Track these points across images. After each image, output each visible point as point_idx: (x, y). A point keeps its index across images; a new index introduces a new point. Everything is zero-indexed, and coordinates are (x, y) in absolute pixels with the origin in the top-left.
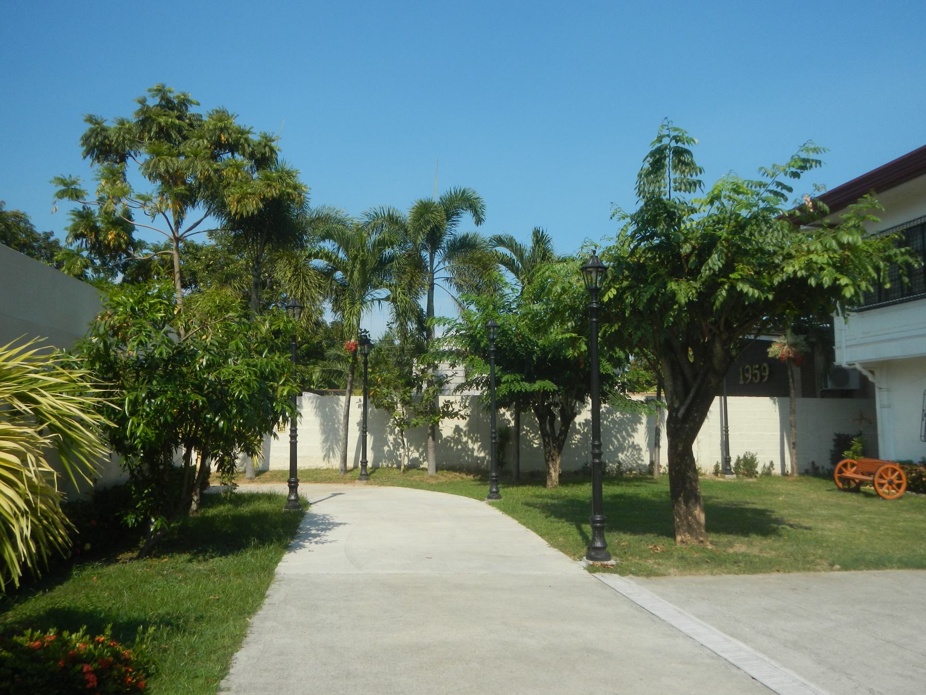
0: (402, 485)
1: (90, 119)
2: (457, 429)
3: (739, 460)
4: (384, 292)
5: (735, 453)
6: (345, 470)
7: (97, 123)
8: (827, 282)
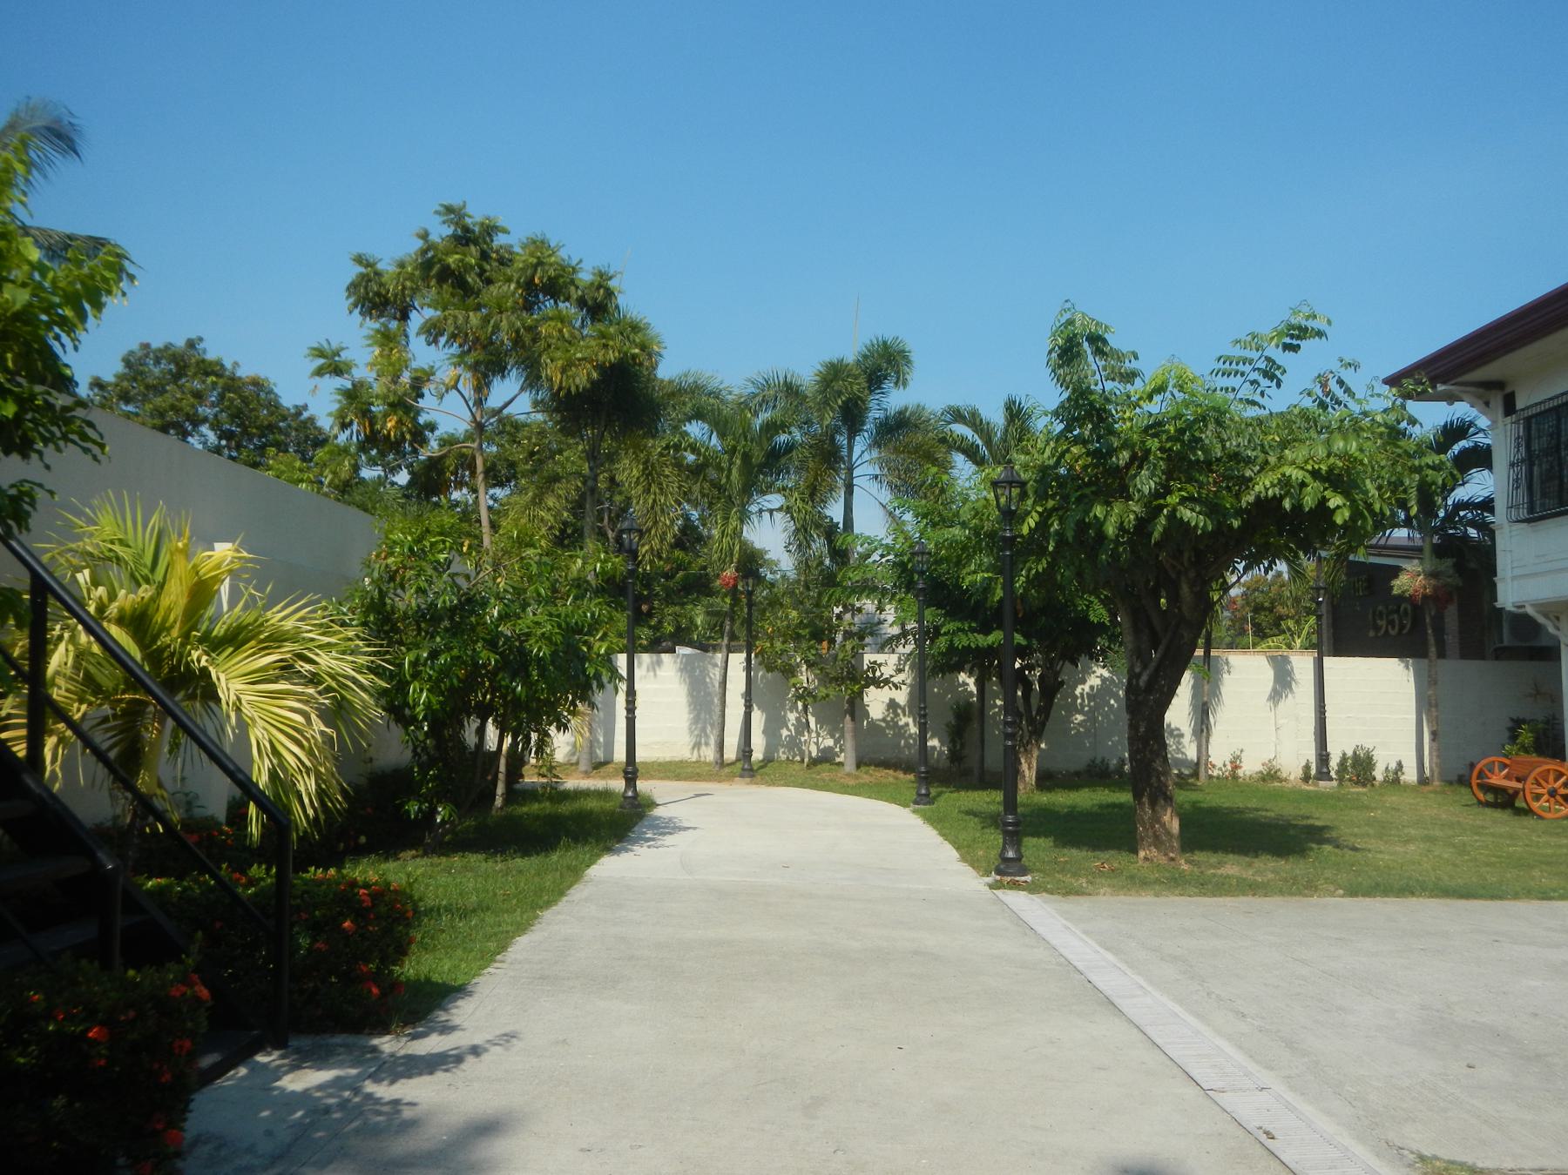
0: (802, 786)
1: (359, 260)
2: (892, 705)
3: (1344, 758)
4: (775, 500)
5: (1335, 752)
6: (721, 763)
7: (368, 265)
8: (1309, 502)
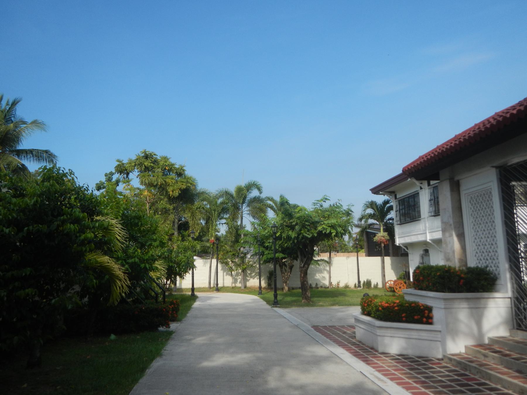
0: (231, 292)
1: (118, 161)
3: (364, 282)
4: (224, 221)
5: (362, 280)
6: (210, 288)
7: (120, 162)
8: (328, 232)
